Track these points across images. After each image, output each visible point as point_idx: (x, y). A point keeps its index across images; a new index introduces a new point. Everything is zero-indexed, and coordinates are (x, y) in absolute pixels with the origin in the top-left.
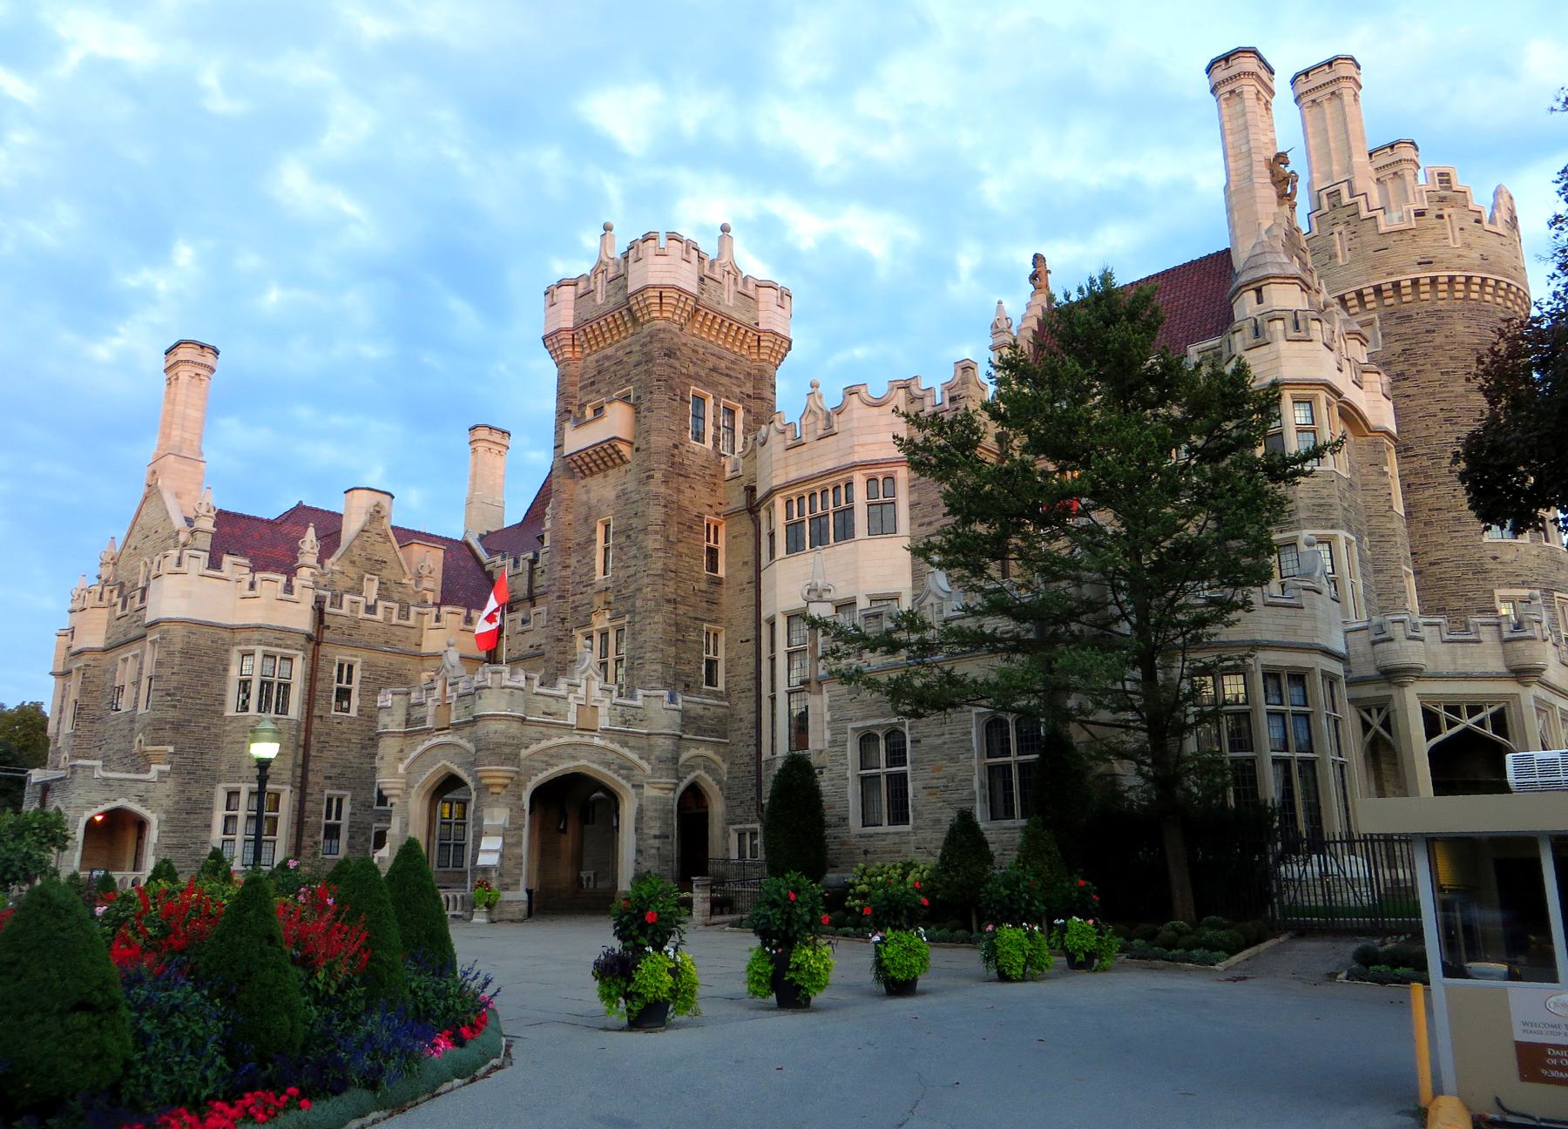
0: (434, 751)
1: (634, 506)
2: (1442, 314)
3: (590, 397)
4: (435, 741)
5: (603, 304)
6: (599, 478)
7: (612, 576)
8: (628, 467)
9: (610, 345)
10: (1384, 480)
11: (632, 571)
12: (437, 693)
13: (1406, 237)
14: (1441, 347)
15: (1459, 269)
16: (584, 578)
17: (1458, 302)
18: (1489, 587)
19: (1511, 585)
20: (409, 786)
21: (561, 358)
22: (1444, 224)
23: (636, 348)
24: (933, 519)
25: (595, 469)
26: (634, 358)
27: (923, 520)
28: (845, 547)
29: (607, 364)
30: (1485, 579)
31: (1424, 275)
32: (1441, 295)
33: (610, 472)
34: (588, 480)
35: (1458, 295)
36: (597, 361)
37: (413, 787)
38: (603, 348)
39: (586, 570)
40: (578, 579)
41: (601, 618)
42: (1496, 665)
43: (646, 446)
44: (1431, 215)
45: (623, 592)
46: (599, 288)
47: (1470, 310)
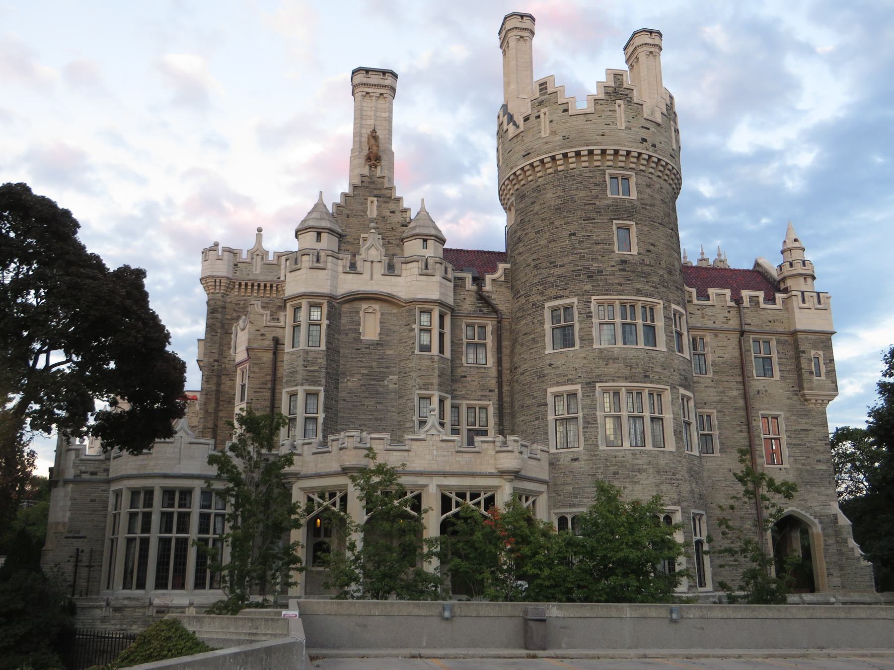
2: (539, 189)
10: (412, 334)
13: (520, 138)
14: (537, 213)
15: (546, 153)
17: (551, 176)
18: (545, 387)
19: (559, 384)
22: (540, 122)
30: (543, 382)
31: (525, 163)
32: (539, 174)
35: (549, 171)
42: (336, 467)
44: (532, 118)
47: (559, 180)
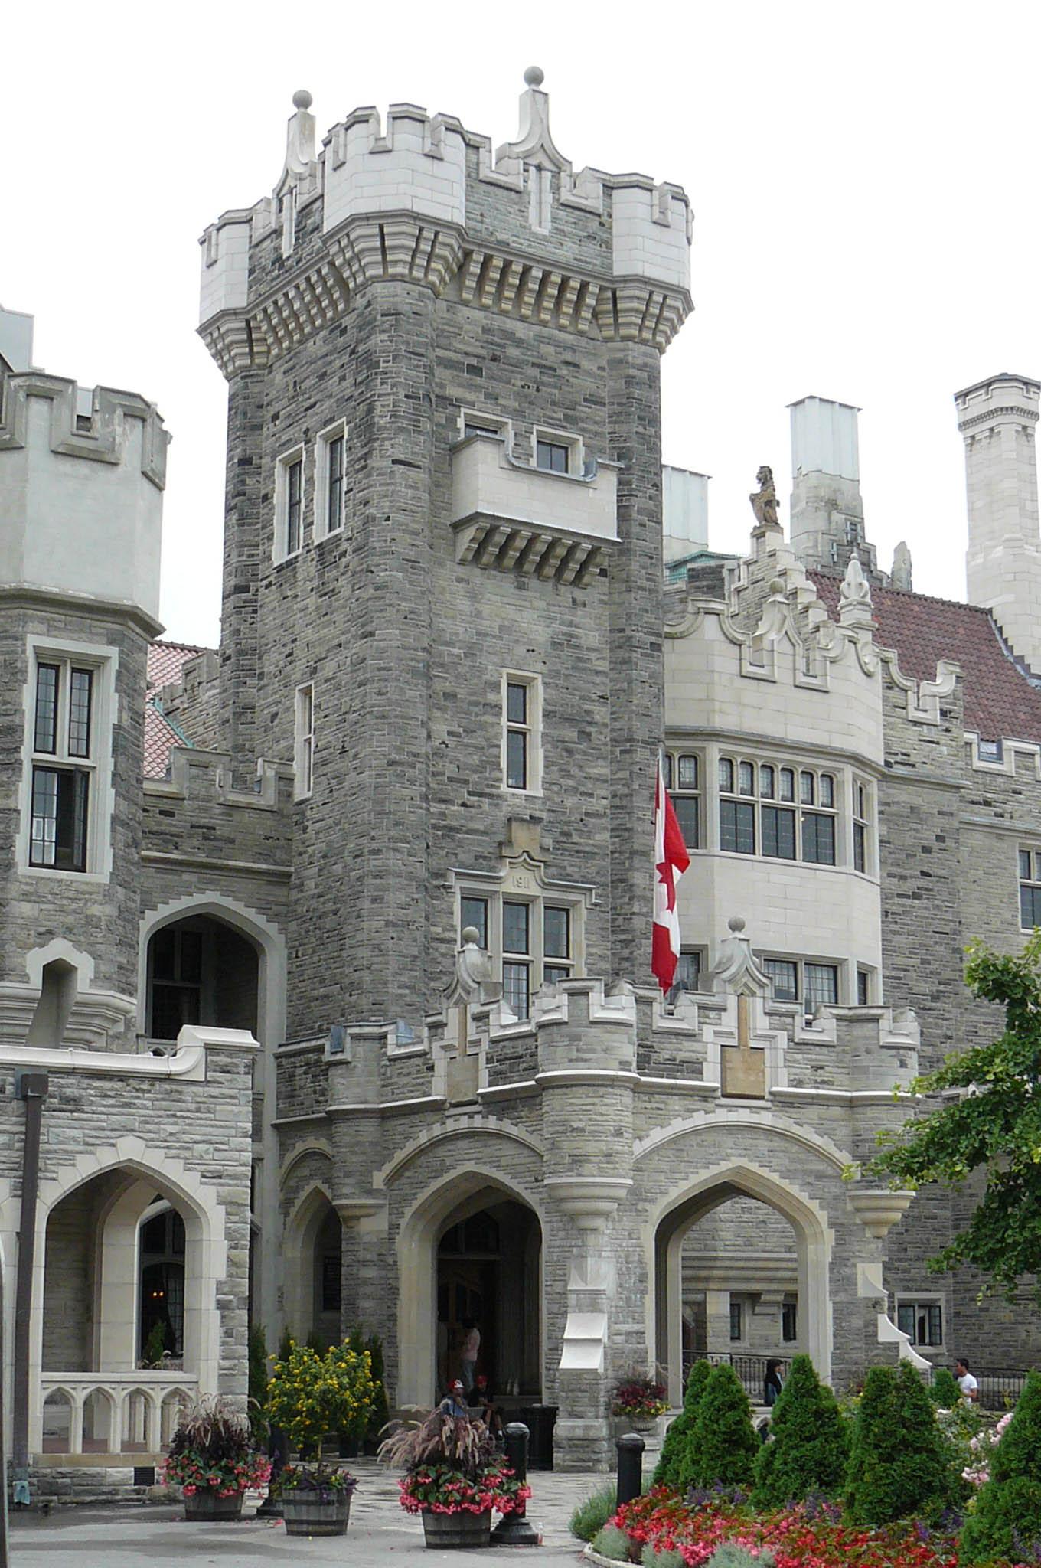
0: (709, 1138)
1: (598, 680)
3: (470, 396)
4: (722, 1116)
5: (545, 238)
6: (506, 583)
7: (546, 798)
8: (579, 594)
9: (523, 319)
11: (599, 805)
12: (729, 1022)
16: (475, 777)
20: (637, 1197)
21: (418, 274)
23: (585, 364)
24: (907, 873)
25: (509, 562)
26: (588, 385)
27: (894, 870)
28: (821, 873)
29: (513, 352)
33: (533, 583)
34: (475, 574)
36: (486, 330)
37: (652, 1201)
38: (504, 313)
39: (475, 759)
40: (451, 770)
41: (521, 873)
43: (648, 585)
45: (575, 839)
46: (534, 198)
